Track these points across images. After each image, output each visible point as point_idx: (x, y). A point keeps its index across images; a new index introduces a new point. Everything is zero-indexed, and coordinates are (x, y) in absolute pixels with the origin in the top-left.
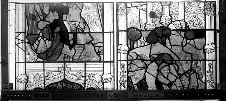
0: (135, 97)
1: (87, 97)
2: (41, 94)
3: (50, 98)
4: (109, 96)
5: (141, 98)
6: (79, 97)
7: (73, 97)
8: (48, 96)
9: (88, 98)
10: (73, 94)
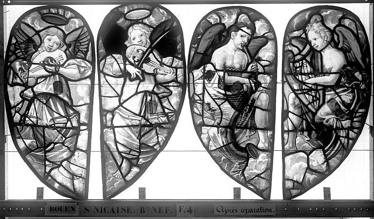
0: (226, 212)
1: (141, 213)
2: (61, 207)
3: (77, 214)
4: (180, 211)
5: (237, 214)
6: (128, 212)
7: (118, 212)
8: (74, 210)
9: (144, 214)
10: (118, 207)
